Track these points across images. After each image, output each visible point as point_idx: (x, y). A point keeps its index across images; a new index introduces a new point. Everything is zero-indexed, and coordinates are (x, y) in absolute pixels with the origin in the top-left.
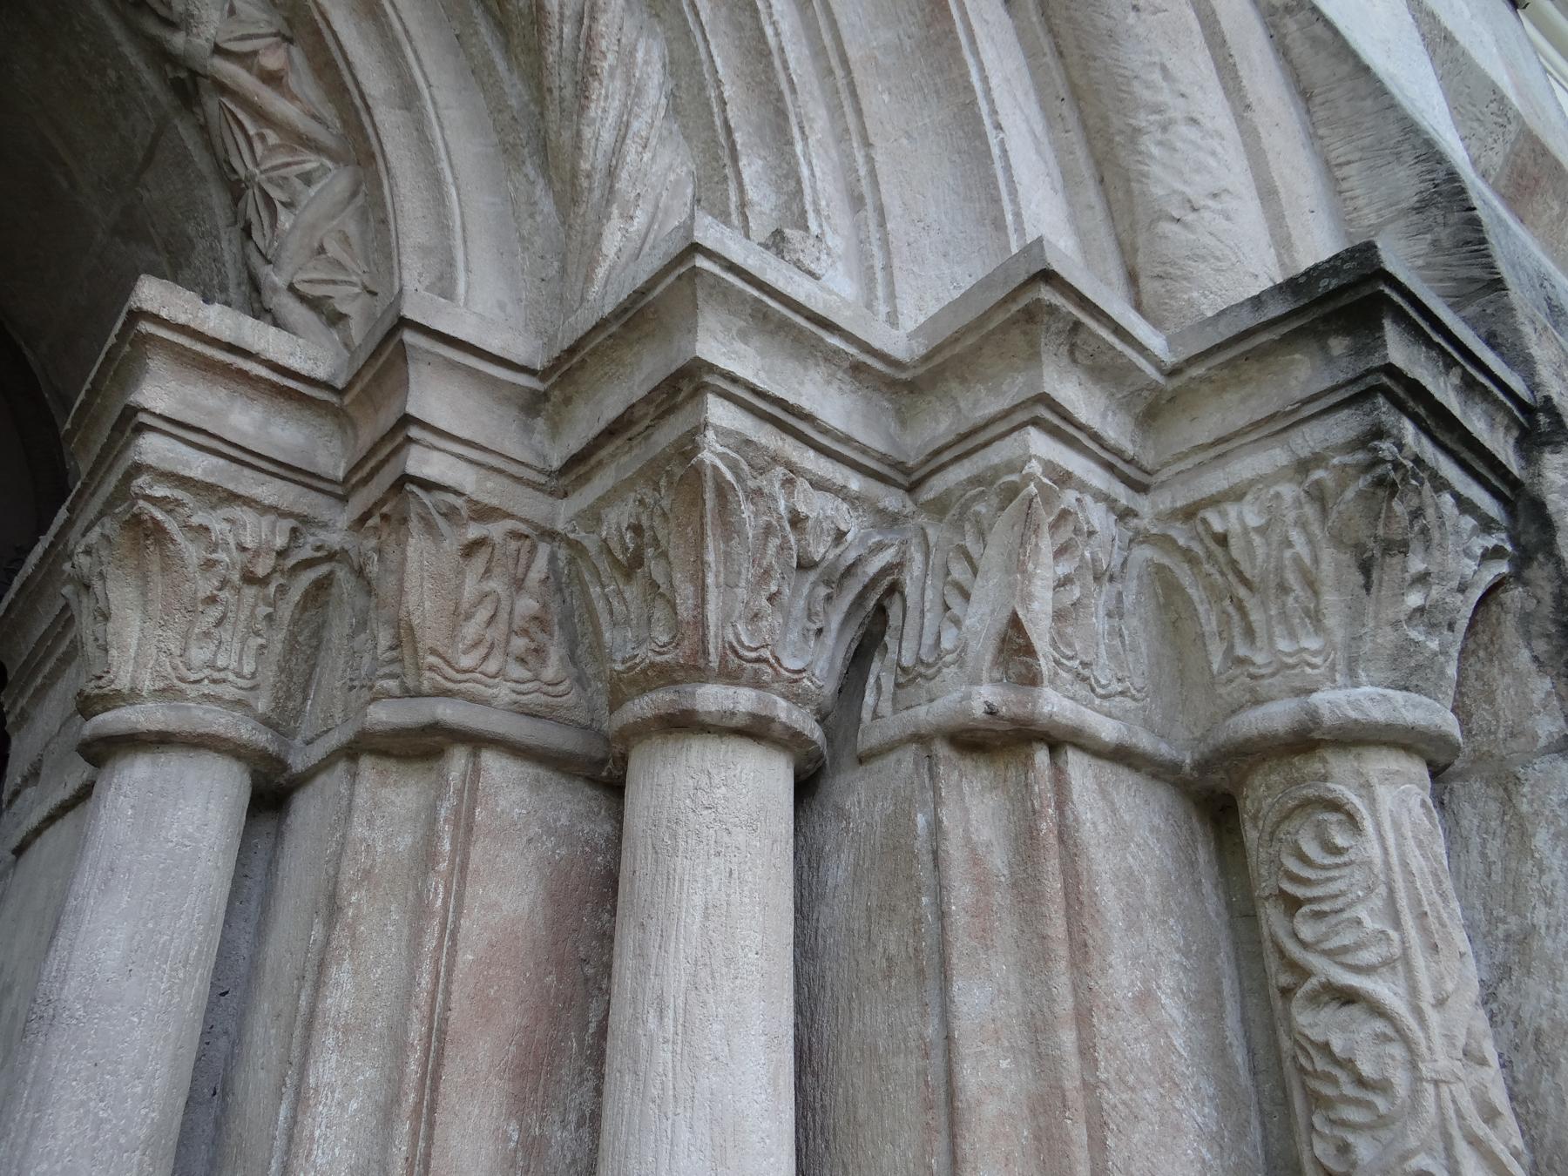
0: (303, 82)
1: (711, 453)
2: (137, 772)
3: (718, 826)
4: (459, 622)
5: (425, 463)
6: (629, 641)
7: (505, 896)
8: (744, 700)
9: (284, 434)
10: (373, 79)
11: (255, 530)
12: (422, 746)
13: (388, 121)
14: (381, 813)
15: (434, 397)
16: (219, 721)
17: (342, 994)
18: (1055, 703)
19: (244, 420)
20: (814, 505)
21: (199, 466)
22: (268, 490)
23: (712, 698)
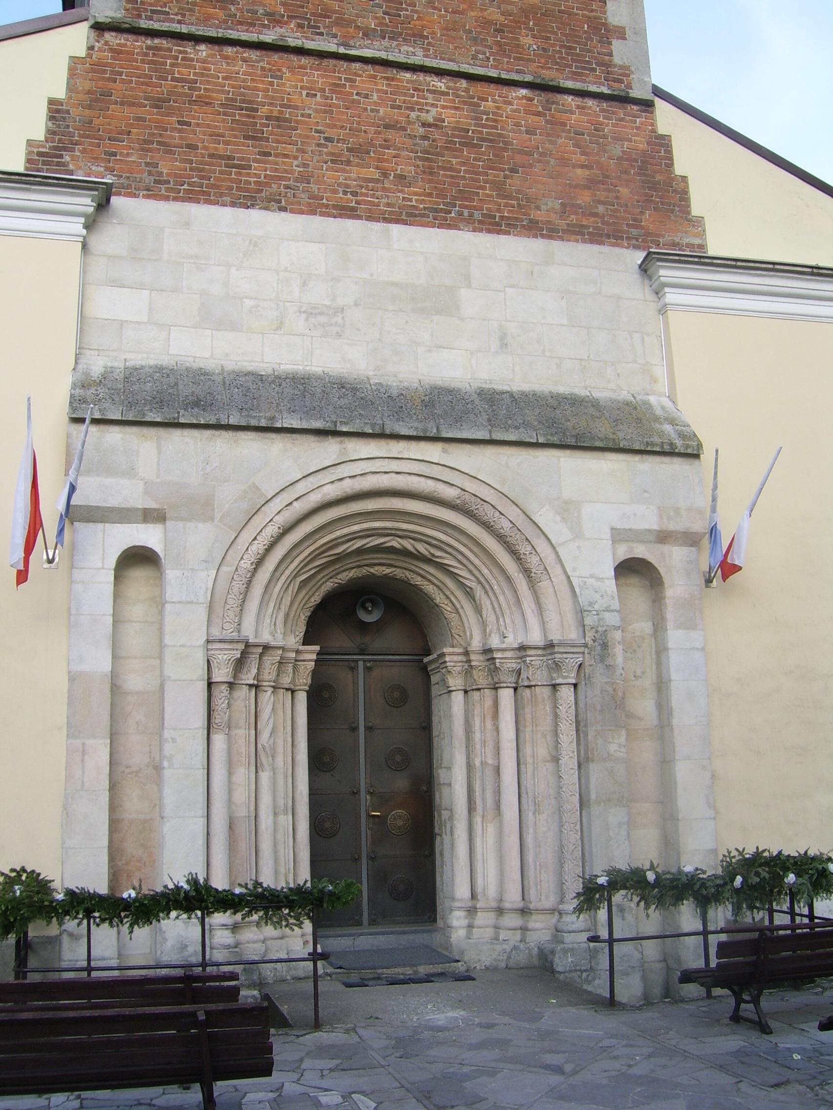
0: (450, 604)
1: (498, 665)
2: (454, 693)
3: (506, 696)
4: (481, 678)
5: (473, 664)
6: (496, 680)
7: (489, 702)
8: (505, 685)
9: (460, 658)
10: (458, 606)
11: (459, 669)
12: (479, 689)
13: (460, 610)
14: (476, 694)
15: (473, 657)
16: (460, 688)
17: (476, 713)
18: (533, 683)
19: (455, 658)
20: (509, 665)
21: (452, 664)
22: (460, 664)
23: (502, 685)
